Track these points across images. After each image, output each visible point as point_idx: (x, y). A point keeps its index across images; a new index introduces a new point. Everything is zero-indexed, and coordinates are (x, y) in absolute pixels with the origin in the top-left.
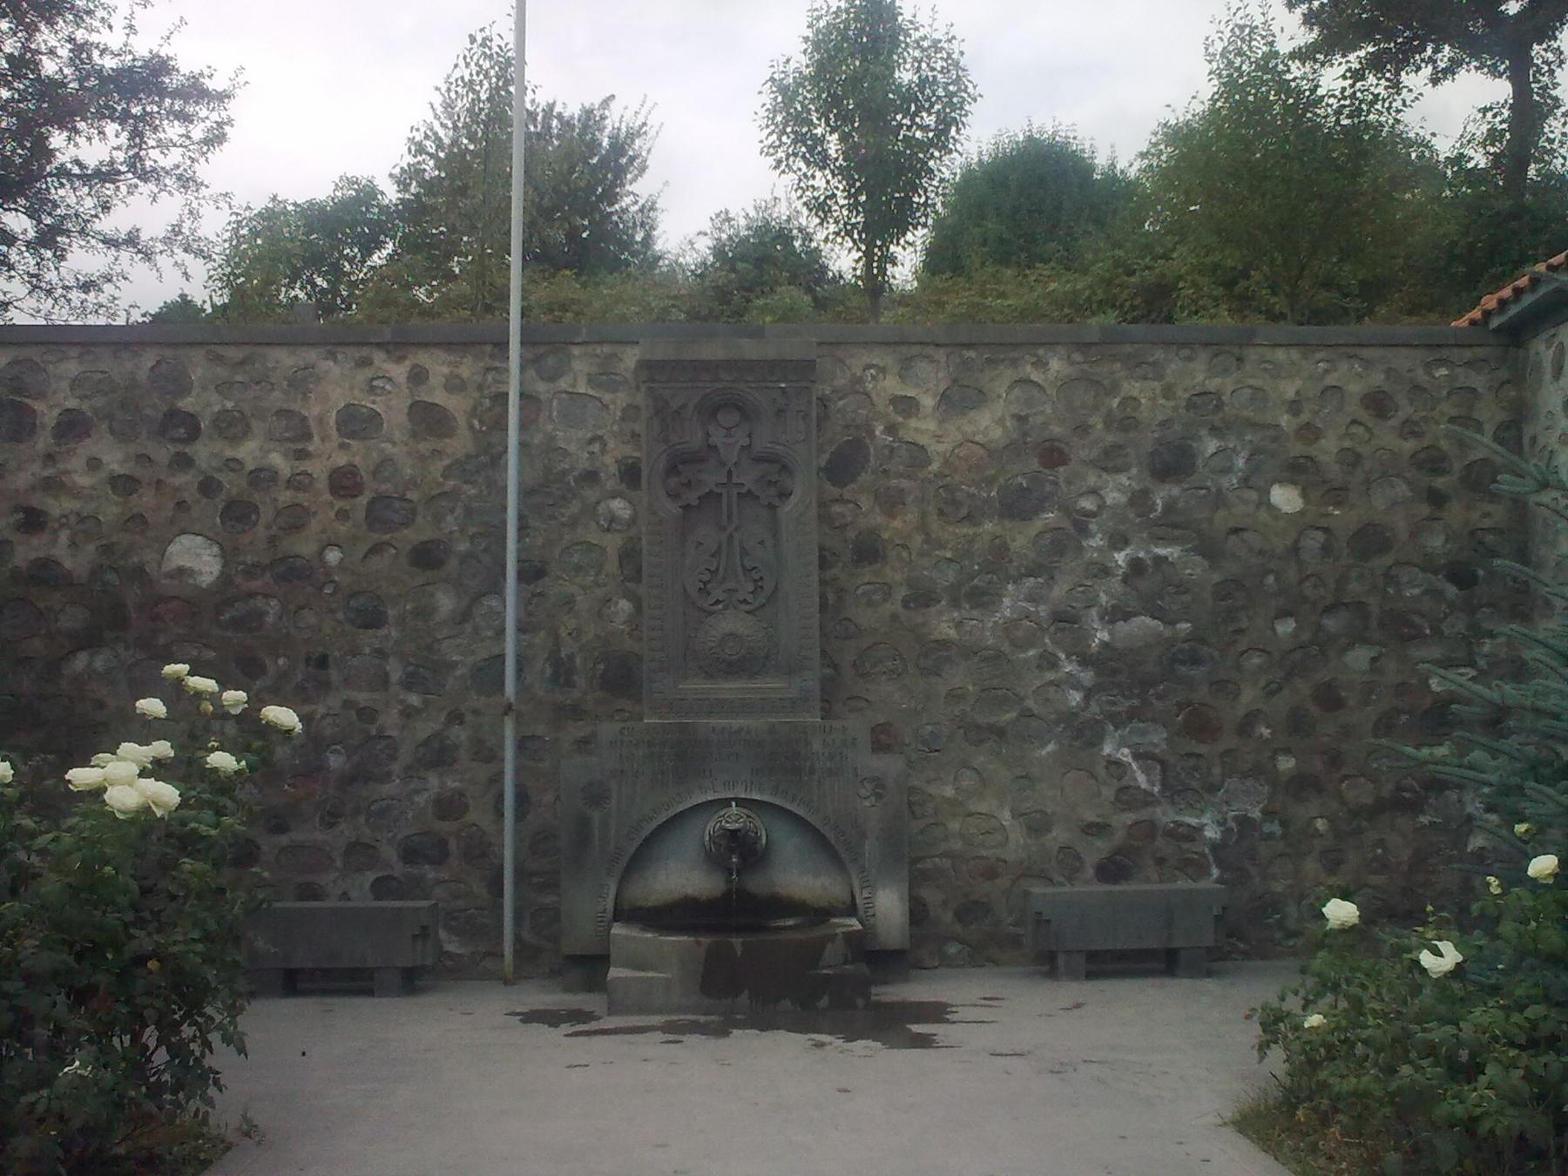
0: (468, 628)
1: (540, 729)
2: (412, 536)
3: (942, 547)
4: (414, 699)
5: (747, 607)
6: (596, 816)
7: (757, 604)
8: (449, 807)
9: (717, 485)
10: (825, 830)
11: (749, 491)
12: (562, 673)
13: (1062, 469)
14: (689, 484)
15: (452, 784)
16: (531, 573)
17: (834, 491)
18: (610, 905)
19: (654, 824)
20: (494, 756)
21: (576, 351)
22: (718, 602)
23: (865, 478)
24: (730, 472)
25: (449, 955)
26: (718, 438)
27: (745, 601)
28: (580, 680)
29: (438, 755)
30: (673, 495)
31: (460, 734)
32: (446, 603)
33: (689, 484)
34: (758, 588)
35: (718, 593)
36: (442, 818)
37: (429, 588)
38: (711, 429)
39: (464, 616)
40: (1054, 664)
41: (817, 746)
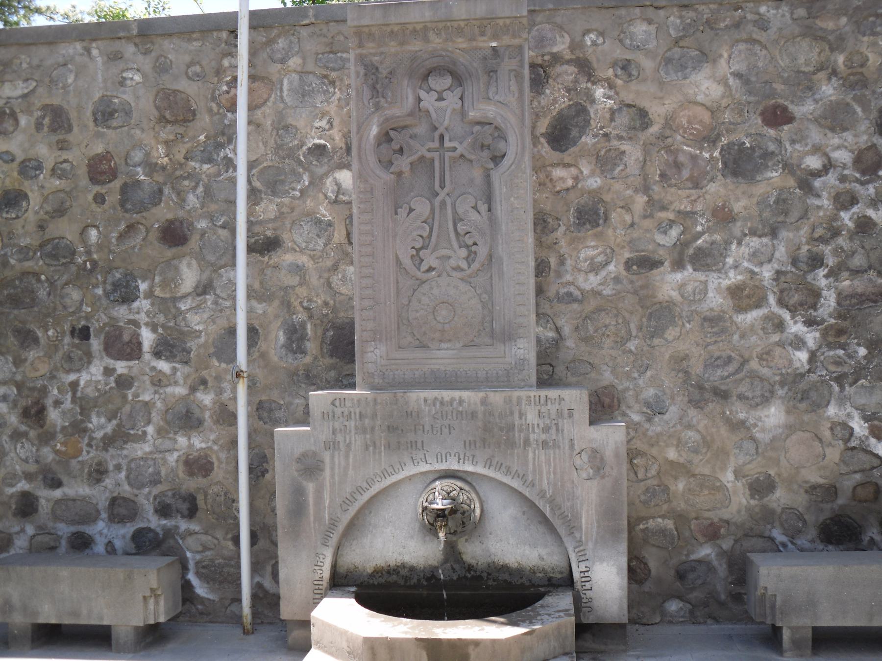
0: (210, 298)
1: (275, 395)
2: (163, 213)
3: (664, 208)
4: (164, 366)
5: (459, 275)
6: (310, 487)
7: (469, 272)
8: (198, 465)
9: (429, 150)
10: (540, 504)
11: (462, 156)
12: (295, 338)
13: (786, 127)
14: (401, 151)
15: (198, 443)
16: (263, 246)
17: (555, 156)
18: (326, 574)
19: (366, 496)
20: (231, 418)
21: (304, 32)
22: (430, 269)
23: (587, 140)
24: (442, 137)
25: (202, 600)
26: (429, 101)
27: (458, 269)
28: (311, 346)
29: (187, 419)
30: (388, 164)
31: (206, 398)
32: (189, 276)
33: (401, 151)
34: (471, 257)
35: (430, 260)
36: (191, 474)
37: (175, 262)
38: (423, 94)
39: (204, 289)
40: (780, 326)
41: (531, 417)
